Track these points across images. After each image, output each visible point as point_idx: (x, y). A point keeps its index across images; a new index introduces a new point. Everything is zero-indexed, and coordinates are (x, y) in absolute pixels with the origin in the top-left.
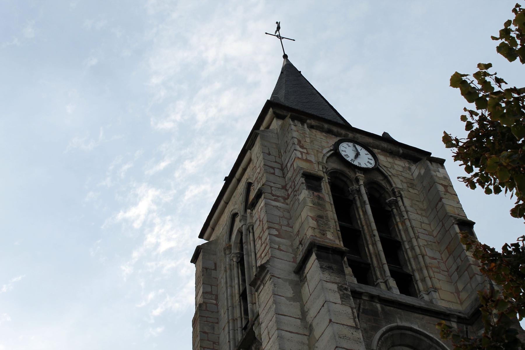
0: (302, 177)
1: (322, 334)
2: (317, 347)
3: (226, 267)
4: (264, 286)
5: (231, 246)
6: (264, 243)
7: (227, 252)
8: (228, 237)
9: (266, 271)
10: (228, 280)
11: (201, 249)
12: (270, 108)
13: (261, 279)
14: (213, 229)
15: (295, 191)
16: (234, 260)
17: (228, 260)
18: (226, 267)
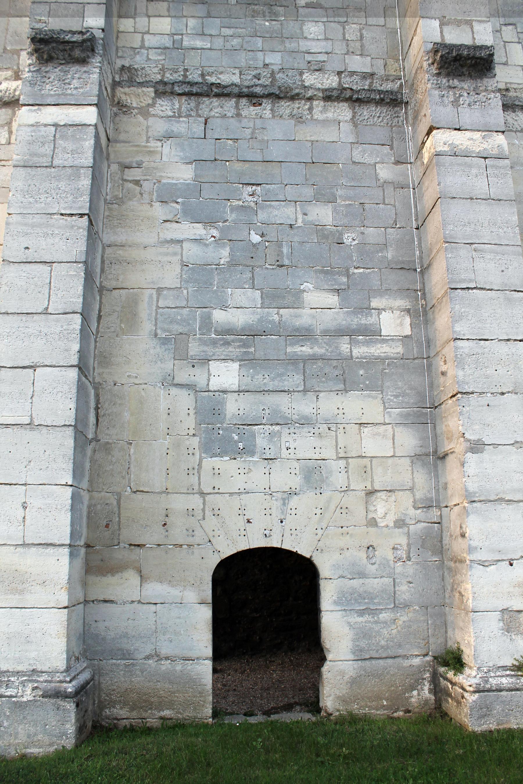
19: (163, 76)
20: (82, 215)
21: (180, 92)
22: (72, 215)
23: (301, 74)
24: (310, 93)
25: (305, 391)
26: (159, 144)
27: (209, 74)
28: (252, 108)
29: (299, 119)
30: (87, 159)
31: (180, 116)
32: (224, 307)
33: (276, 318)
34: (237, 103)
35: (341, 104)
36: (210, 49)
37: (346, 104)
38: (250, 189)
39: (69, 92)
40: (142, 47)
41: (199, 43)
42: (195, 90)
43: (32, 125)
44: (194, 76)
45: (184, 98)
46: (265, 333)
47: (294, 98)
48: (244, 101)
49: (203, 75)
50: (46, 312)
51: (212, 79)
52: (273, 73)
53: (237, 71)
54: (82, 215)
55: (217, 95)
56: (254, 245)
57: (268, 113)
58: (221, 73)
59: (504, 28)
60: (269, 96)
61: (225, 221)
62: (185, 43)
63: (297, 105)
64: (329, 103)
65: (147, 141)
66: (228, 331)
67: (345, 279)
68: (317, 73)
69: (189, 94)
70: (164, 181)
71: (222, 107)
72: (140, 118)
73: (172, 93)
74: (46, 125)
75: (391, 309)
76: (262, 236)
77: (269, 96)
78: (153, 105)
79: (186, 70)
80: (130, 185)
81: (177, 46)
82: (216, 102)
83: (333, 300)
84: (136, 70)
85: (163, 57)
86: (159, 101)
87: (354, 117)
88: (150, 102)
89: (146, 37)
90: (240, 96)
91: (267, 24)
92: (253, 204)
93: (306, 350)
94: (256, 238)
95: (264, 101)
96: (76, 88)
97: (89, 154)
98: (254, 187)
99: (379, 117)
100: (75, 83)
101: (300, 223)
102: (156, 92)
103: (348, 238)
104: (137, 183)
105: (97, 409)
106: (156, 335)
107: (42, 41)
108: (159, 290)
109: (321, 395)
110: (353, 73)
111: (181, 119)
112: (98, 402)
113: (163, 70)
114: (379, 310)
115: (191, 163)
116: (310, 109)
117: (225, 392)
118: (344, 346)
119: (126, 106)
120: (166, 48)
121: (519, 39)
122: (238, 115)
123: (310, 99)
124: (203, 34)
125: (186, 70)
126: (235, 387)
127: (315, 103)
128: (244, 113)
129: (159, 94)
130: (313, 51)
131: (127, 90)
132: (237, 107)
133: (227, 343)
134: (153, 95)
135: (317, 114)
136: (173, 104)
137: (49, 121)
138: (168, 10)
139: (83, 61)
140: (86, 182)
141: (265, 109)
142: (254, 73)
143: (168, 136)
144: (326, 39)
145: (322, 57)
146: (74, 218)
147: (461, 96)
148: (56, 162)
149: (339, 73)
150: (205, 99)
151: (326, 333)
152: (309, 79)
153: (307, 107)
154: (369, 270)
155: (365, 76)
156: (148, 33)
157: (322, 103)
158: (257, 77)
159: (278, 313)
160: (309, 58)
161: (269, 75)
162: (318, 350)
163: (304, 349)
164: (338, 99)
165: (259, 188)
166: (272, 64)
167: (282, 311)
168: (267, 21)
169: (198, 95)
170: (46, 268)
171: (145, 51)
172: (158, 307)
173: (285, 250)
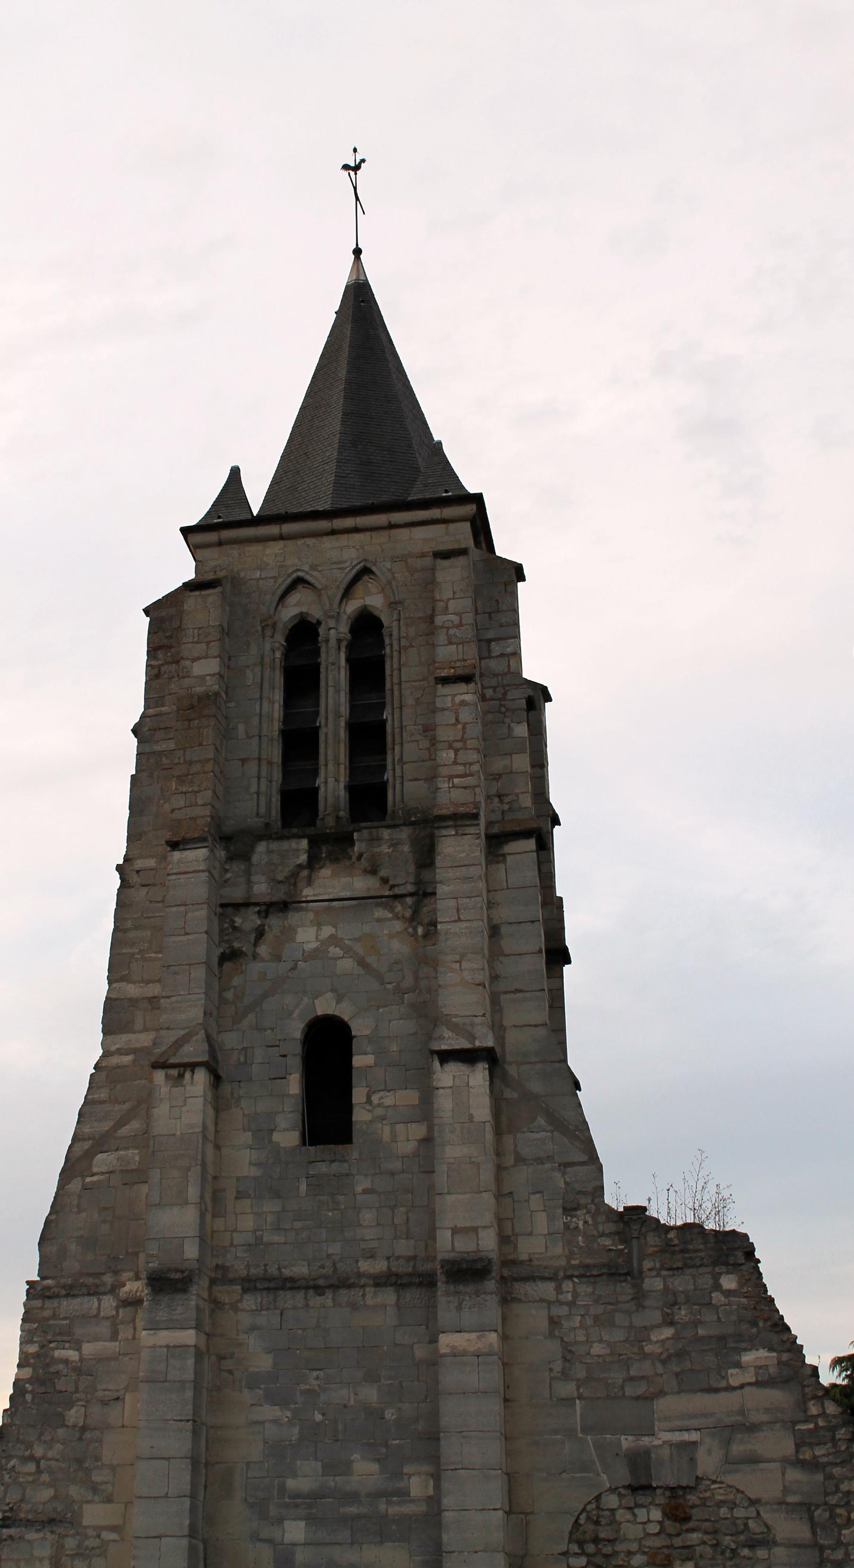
0: (525, 698)
1: (519, 955)
2: (501, 962)
3: (262, 657)
4: (456, 834)
5: (275, 624)
6: (464, 765)
7: (269, 633)
8: (274, 604)
9: (475, 822)
10: (266, 686)
11: (221, 585)
12: (472, 503)
13: (459, 823)
14: (220, 544)
15: (504, 706)
16: (278, 655)
17: (268, 646)
18: (262, 657)
19: (248, 1271)
20: (188, 1421)
21: (261, 1288)
22: (181, 1420)
23: (357, 1261)
24: (363, 1281)
25: (352, 1543)
26: (246, 1336)
27: (285, 1267)
28: (318, 1298)
29: (354, 1307)
30: (190, 1375)
31: (262, 1310)
32: (295, 1476)
33: (332, 1484)
34: (306, 1294)
35: (388, 1288)
36: (285, 1243)
37: (392, 1288)
38: (315, 1374)
39: (175, 1317)
40: (232, 1245)
41: (276, 1238)
42: (272, 1285)
43: (151, 1347)
44: (273, 1270)
45: (264, 1293)
46: (324, 1497)
47: (350, 1286)
48: (311, 1292)
49: (279, 1269)
50: (166, 1496)
51: (287, 1272)
52: (334, 1264)
53: (306, 1263)
54: (188, 1421)
55: (291, 1288)
56: (318, 1424)
57: (329, 1302)
58: (293, 1266)
59: (532, 1196)
60: (331, 1286)
61: (296, 1403)
62: (265, 1239)
63: (353, 1293)
64: (379, 1288)
65: (237, 1334)
66: (298, 1496)
67: (384, 1450)
68: (370, 1260)
69: (268, 1289)
70: (251, 1370)
71: (294, 1299)
72: (231, 1312)
73: (256, 1289)
74: (161, 1347)
75: (419, 1474)
76: (323, 1415)
77: (331, 1286)
78: (241, 1300)
79: (266, 1265)
80: (226, 1375)
81: (259, 1241)
82: (289, 1294)
83: (374, 1467)
84: (228, 1267)
85: (248, 1254)
86: (246, 1296)
87: (398, 1300)
88: (239, 1297)
89: (235, 1235)
90: (307, 1288)
91: (330, 1214)
92: (317, 1388)
93: (353, 1510)
94: (318, 1417)
95: (327, 1291)
96: (180, 1314)
97: (191, 1370)
98: (318, 1372)
99: (419, 1299)
100: (180, 1309)
101: (352, 1403)
102: (243, 1289)
103: (390, 1414)
104: (230, 1372)
105: (205, 1559)
106: (246, 1500)
107: (154, 1279)
108: (248, 1464)
109: (364, 1546)
110: (398, 1258)
111: (263, 1312)
112: (205, 1554)
113: (248, 1267)
114: (410, 1476)
115: (269, 1353)
116: (364, 1296)
117: (295, 1545)
118: (382, 1507)
119: (220, 1303)
120: (250, 1245)
121: (545, 1206)
122: (307, 1306)
123: (364, 1286)
124: (279, 1229)
125: (266, 1265)
126: (302, 1541)
127: (367, 1289)
128: (311, 1304)
129: (245, 1291)
130: (367, 1238)
131: (220, 1288)
132: (306, 1298)
133: (297, 1506)
134: (240, 1291)
135: (370, 1301)
136: (256, 1298)
137: (163, 1342)
138: (251, 1207)
139: (185, 1291)
140: (189, 1394)
141: (327, 1298)
142: (319, 1264)
143: (253, 1328)
144: (378, 1225)
145: (374, 1244)
146: (183, 1423)
147: (464, 1300)
148: (169, 1378)
149: (388, 1258)
150: (281, 1292)
151: (368, 1495)
152: (365, 1266)
153: (361, 1294)
154: (403, 1441)
155: (409, 1259)
156: (235, 1230)
157: (373, 1289)
158: (323, 1267)
159: (334, 1480)
160: (363, 1245)
161: (331, 1265)
162: (363, 1510)
163: (352, 1509)
164: (385, 1285)
165: (322, 1373)
166: (333, 1254)
167: (338, 1479)
168: (330, 1211)
169: (275, 1289)
170: (165, 1463)
171: (233, 1249)
172: (247, 1478)
173: (340, 1427)
